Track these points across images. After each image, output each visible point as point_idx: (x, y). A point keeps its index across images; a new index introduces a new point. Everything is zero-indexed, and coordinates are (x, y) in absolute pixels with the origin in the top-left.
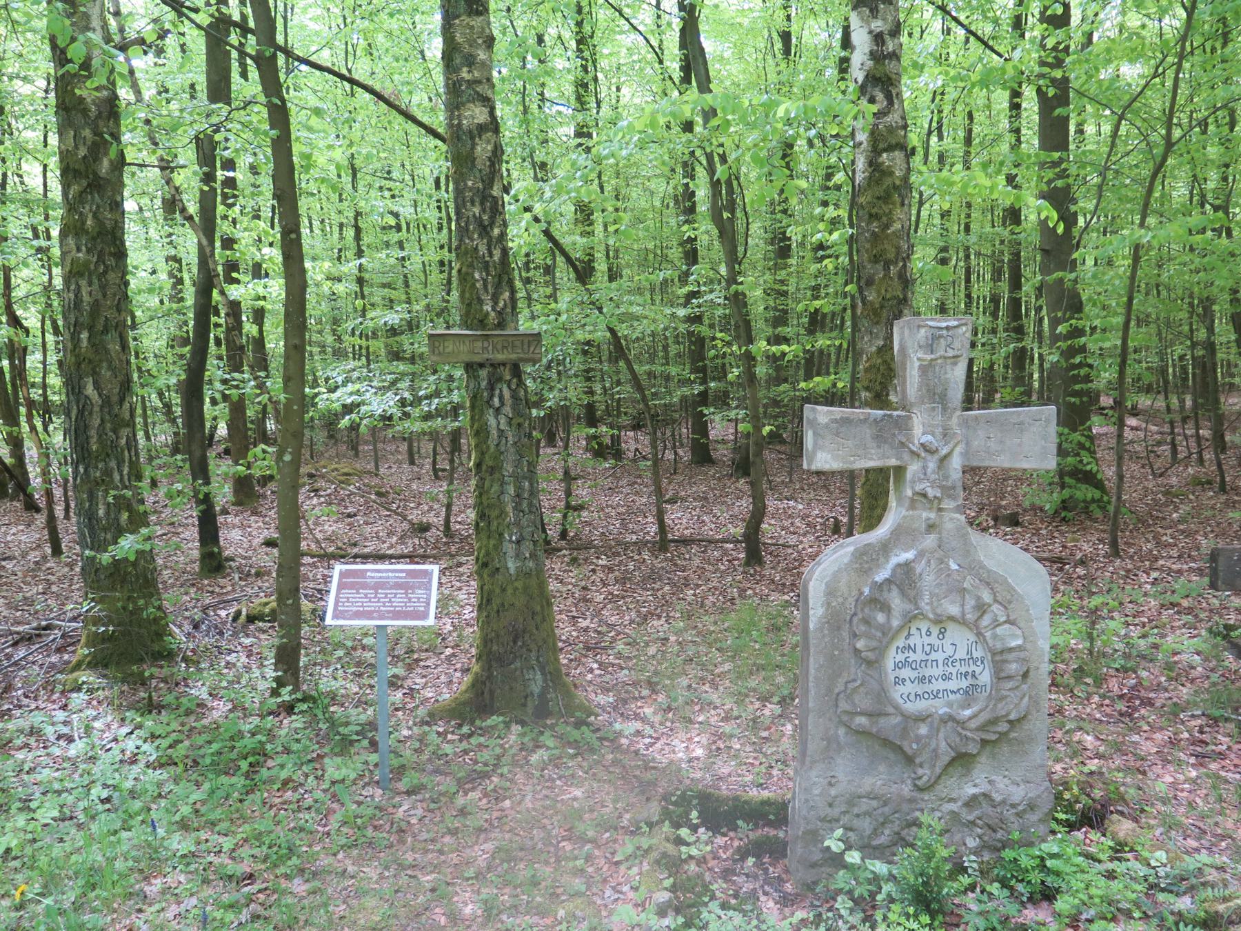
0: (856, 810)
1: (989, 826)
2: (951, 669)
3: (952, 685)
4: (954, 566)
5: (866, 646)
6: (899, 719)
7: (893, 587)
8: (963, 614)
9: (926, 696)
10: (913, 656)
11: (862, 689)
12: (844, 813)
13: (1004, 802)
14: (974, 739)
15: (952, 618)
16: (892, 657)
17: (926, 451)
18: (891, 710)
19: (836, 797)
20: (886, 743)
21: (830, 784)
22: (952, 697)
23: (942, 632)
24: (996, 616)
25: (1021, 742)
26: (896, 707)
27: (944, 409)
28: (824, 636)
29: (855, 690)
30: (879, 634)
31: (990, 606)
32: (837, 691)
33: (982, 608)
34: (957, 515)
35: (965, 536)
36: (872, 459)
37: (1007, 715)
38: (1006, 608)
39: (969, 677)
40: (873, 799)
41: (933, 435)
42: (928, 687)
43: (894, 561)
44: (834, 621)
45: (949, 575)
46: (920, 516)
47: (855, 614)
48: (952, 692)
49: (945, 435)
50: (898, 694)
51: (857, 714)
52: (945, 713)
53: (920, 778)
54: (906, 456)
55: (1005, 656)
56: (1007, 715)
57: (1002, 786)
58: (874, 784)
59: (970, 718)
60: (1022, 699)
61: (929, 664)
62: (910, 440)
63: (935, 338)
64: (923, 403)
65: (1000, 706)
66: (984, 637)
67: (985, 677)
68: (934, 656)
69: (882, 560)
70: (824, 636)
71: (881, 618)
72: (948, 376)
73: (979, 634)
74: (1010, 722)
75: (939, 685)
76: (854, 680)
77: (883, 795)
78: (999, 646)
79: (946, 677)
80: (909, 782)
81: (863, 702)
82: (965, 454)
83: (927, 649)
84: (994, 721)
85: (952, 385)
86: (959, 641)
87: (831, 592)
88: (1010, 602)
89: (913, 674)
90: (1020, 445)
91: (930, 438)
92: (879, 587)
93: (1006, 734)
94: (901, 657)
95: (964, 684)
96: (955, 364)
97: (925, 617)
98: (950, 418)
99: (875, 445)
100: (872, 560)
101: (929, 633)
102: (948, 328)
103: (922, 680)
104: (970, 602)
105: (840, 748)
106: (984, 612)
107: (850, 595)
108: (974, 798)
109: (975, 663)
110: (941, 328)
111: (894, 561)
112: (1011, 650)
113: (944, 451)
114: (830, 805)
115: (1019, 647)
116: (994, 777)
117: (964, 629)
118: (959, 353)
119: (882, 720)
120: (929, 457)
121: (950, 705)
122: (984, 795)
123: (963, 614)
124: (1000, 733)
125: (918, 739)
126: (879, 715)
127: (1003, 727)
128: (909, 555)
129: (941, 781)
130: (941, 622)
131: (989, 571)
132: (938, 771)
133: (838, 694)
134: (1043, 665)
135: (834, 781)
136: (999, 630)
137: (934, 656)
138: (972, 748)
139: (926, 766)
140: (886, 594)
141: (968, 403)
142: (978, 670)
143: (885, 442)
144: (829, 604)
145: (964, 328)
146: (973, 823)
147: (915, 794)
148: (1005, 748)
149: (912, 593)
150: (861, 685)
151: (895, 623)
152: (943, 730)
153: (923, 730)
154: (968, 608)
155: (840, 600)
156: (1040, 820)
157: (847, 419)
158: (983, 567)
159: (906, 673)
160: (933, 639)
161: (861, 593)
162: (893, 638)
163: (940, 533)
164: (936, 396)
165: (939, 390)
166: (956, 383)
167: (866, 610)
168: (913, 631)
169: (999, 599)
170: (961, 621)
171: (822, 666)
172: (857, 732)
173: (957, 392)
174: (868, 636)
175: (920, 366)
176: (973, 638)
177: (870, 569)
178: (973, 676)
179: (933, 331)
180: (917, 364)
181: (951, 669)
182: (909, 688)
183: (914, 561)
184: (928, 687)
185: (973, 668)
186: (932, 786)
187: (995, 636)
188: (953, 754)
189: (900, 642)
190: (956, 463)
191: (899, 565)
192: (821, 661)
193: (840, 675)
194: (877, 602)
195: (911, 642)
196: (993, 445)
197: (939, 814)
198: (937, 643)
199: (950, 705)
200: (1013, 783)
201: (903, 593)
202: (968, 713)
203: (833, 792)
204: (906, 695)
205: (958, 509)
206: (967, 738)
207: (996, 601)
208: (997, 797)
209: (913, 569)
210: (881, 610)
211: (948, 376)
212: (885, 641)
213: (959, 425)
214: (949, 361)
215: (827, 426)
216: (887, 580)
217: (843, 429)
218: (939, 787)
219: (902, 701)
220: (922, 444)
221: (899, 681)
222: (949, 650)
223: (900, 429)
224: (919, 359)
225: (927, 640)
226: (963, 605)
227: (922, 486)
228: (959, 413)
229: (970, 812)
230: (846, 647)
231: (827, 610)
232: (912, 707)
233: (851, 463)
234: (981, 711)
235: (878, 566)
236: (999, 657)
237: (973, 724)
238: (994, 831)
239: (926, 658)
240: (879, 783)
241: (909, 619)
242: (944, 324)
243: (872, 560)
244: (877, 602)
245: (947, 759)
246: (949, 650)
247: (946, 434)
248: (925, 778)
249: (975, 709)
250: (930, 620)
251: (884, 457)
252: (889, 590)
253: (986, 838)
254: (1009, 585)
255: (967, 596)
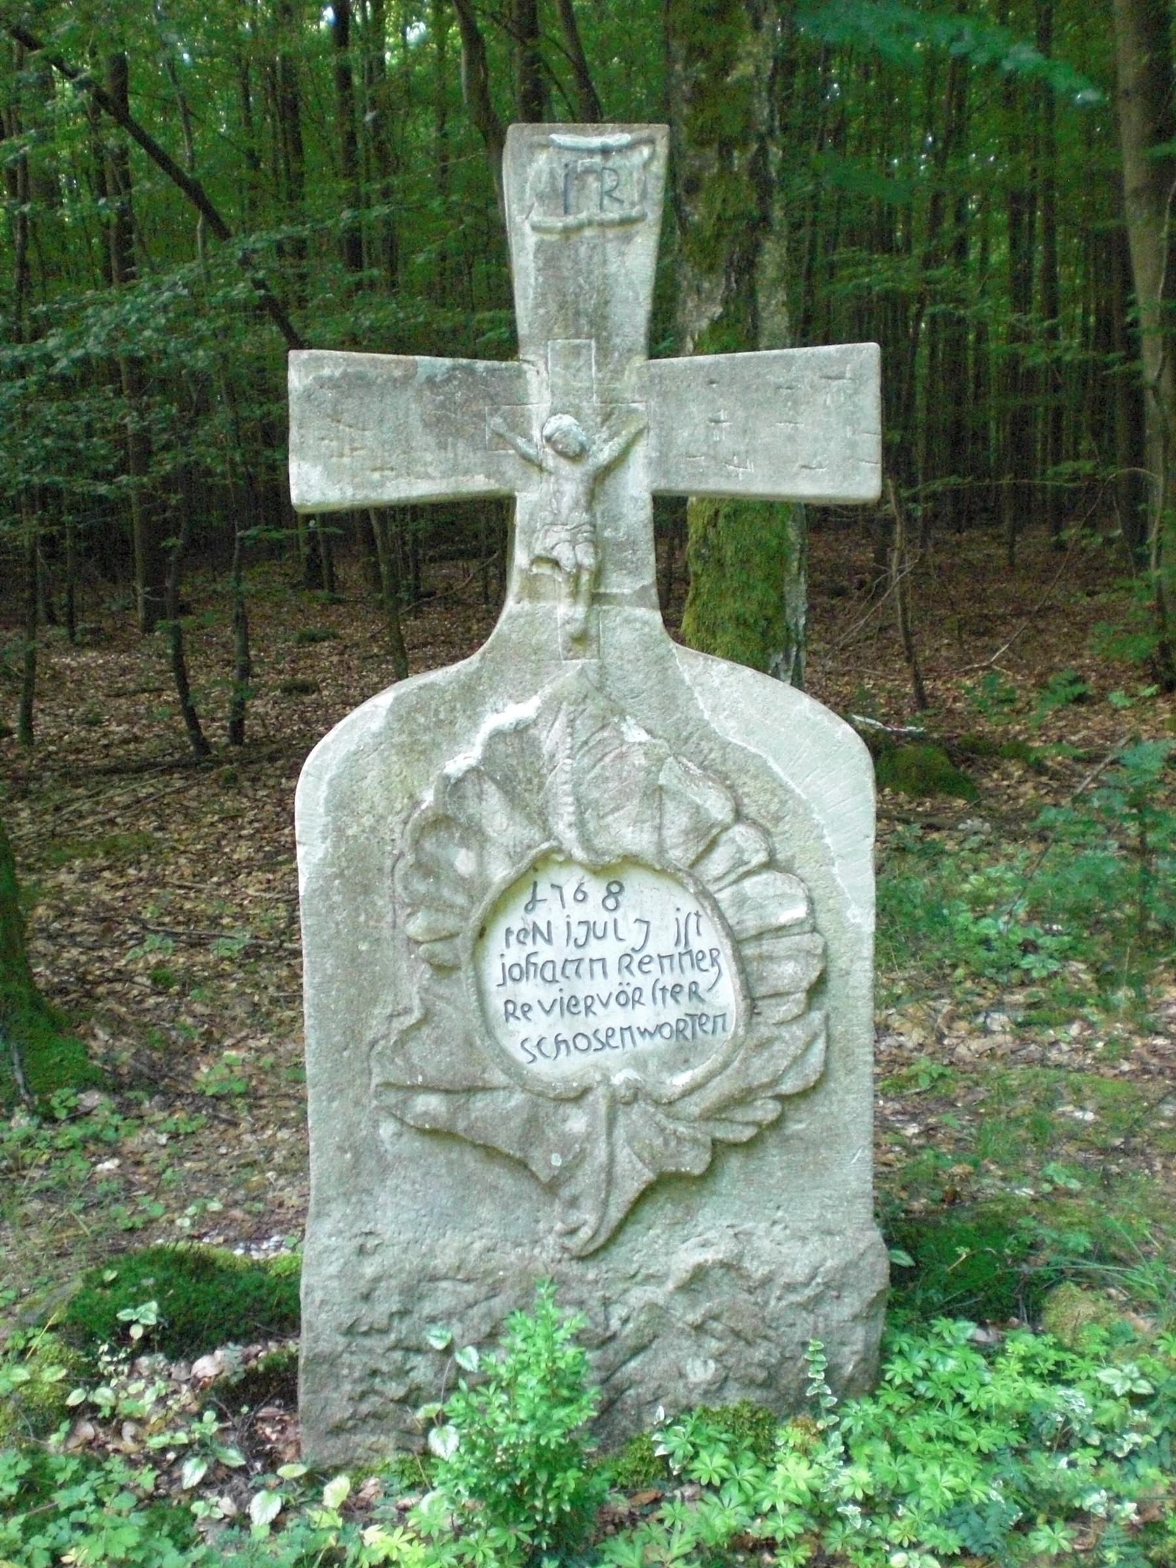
0: (427, 1308)
1: (737, 1334)
2: (638, 980)
3: (643, 1016)
4: (635, 734)
5: (429, 930)
6: (518, 1098)
7: (490, 788)
8: (661, 850)
9: (582, 1043)
10: (545, 953)
11: (426, 1030)
12: (403, 1313)
13: (767, 1281)
14: (695, 1141)
15: (632, 860)
16: (501, 953)
17: (562, 454)
18: (498, 1077)
19: (377, 1280)
20: (490, 1152)
21: (361, 1251)
22: (644, 1044)
23: (615, 890)
24: (741, 851)
25: (810, 1145)
26: (512, 1069)
27: (604, 351)
28: (331, 909)
29: (406, 1035)
30: (461, 900)
31: (726, 828)
32: (369, 1035)
33: (707, 838)
34: (641, 612)
35: (661, 661)
36: (428, 476)
37: (775, 1081)
38: (766, 833)
39: (683, 998)
40: (468, 1281)
41: (577, 416)
42: (586, 1024)
43: (491, 722)
44: (356, 873)
45: (622, 756)
46: (549, 614)
47: (401, 855)
48: (644, 1032)
49: (607, 417)
50: (517, 1037)
51: (414, 1089)
52: (628, 1083)
53: (573, 1232)
54: (512, 469)
55: (767, 946)
56: (775, 1081)
57: (766, 1244)
58: (467, 1249)
59: (688, 1092)
60: (809, 1045)
61: (585, 966)
62: (518, 424)
63: (575, 177)
64: (549, 335)
65: (757, 1062)
66: (715, 905)
67: (726, 995)
68: (595, 949)
69: (462, 722)
70: (331, 909)
71: (464, 861)
72: (612, 268)
73: (704, 894)
74: (781, 1098)
75: (616, 1017)
76: (407, 1011)
77: (487, 1273)
78: (751, 923)
79: (628, 999)
80: (550, 1240)
81: (430, 1057)
82: (660, 464)
83: (580, 932)
84: (745, 1098)
85: (622, 292)
86: (657, 911)
87: (342, 802)
88: (777, 819)
89: (548, 994)
90: (791, 438)
91: (567, 421)
92: (454, 788)
93: (777, 1124)
94: (515, 954)
95: (672, 1013)
96: (628, 239)
97: (569, 860)
98: (617, 373)
99: (431, 440)
100: (440, 723)
101: (581, 896)
102: (605, 151)
103: (570, 1006)
104: (677, 821)
105: (385, 1169)
106: (712, 845)
107: (390, 810)
108: (700, 1274)
109: (696, 963)
110: (591, 152)
111: (491, 722)
112: (780, 931)
113: (605, 453)
114: (366, 1297)
115: (800, 923)
116: (748, 1225)
117: (664, 884)
118: (634, 212)
119: (480, 1104)
120: (565, 467)
121: (639, 1062)
122: (726, 1266)
123: (661, 850)
124: (758, 1124)
125: (565, 1143)
126: (471, 1090)
127: (766, 1110)
128: (527, 709)
129: (622, 1238)
130: (612, 870)
131: (725, 746)
132: (615, 1214)
133: (373, 1044)
134: (858, 966)
135: (371, 1243)
136: (748, 884)
137: (595, 949)
138: (693, 1162)
139: (587, 1203)
140: (472, 806)
141: (663, 337)
142: (704, 980)
143: (458, 434)
144: (340, 831)
145: (646, 151)
146: (699, 1328)
147: (575, 1269)
148: (774, 1158)
149: (536, 800)
150: (425, 1020)
151: (500, 872)
152: (622, 1120)
153: (577, 1122)
154: (672, 834)
155: (368, 821)
156: (855, 1318)
157: (361, 377)
158: (710, 736)
159: (529, 991)
160: (593, 910)
161: (416, 804)
162: (498, 908)
163: (599, 654)
164: (586, 319)
165: (589, 305)
166: (631, 285)
167: (428, 845)
168: (544, 890)
169: (751, 810)
170: (662, 869)
171: (331, 979)
172: (422, 1132)
173: (633, 312)
174: (432, 903)
175: (540, 247)
176: (689, 905)
177: (435, 745)
178: (694, 994)
179: (567, 157)
180: (531, 239)
181: (638, 980)
182: (539, 1026)
183: (535, 723)
184: (586, 1024)
185: (691, 975)
186: (604, 1247)
187: (741, 902)
188: (649, 1175)
189: (515, 919)
190: (636, 488)
191: (498, 735)
192: (329, 963)
193: (374, 1002)
194: (449, 821)
195: (540, 916)
196: (725, 440)
197: (624, 1312)
198: (601, 917)
199: (639, 1062)
200: (792, 1237)
201: (513, 798)
202: (682, 1080)
203: (369, 1269)
204: (533, 1040)
205: (640, 598)
206: (680, 1140)
207: (739, 816)
208: (757, 1270)
209: (535, 744)
210: (464, 843)
211: (612, 268)
212: (476, 914)
213: (642, 389)
214: (610, 233)
215: (308, 395)
216: (473, 770)
217: (350, 404)
218: (619, 1252)
219: (522, 1057)
220: (549, 439)
221: (519, 1010)
222: (633, 936)
223: (492, 398)
224: (535, 228)
225: (578, 913)
226: (659, 828)
227: (549, 542)
228: (639, 361)
229: (693, 1305)
230: (387, 933)
231: (336, 846)
232: (557, 1069)
233: (375, 486)
234: (711, 1076)
235: (454, 739)
236: (747, 947)
237: (693, 1107)
238: (749, 1343)
239: (578, 954)
240: (478, 1246)
241: (533, 869)
242: (596, 141)
243: (440, 723)
244: (449, 821)
245: (631, 1188)
246: (633, 936)
247: (610, 412)
248: (585, 1233)
249: (697, 1072)
250: (581, 864)
251: (454, 469)
252: (480, 796)
253: (731, 1361)
254: (774, 778)
255: (670, 805)
